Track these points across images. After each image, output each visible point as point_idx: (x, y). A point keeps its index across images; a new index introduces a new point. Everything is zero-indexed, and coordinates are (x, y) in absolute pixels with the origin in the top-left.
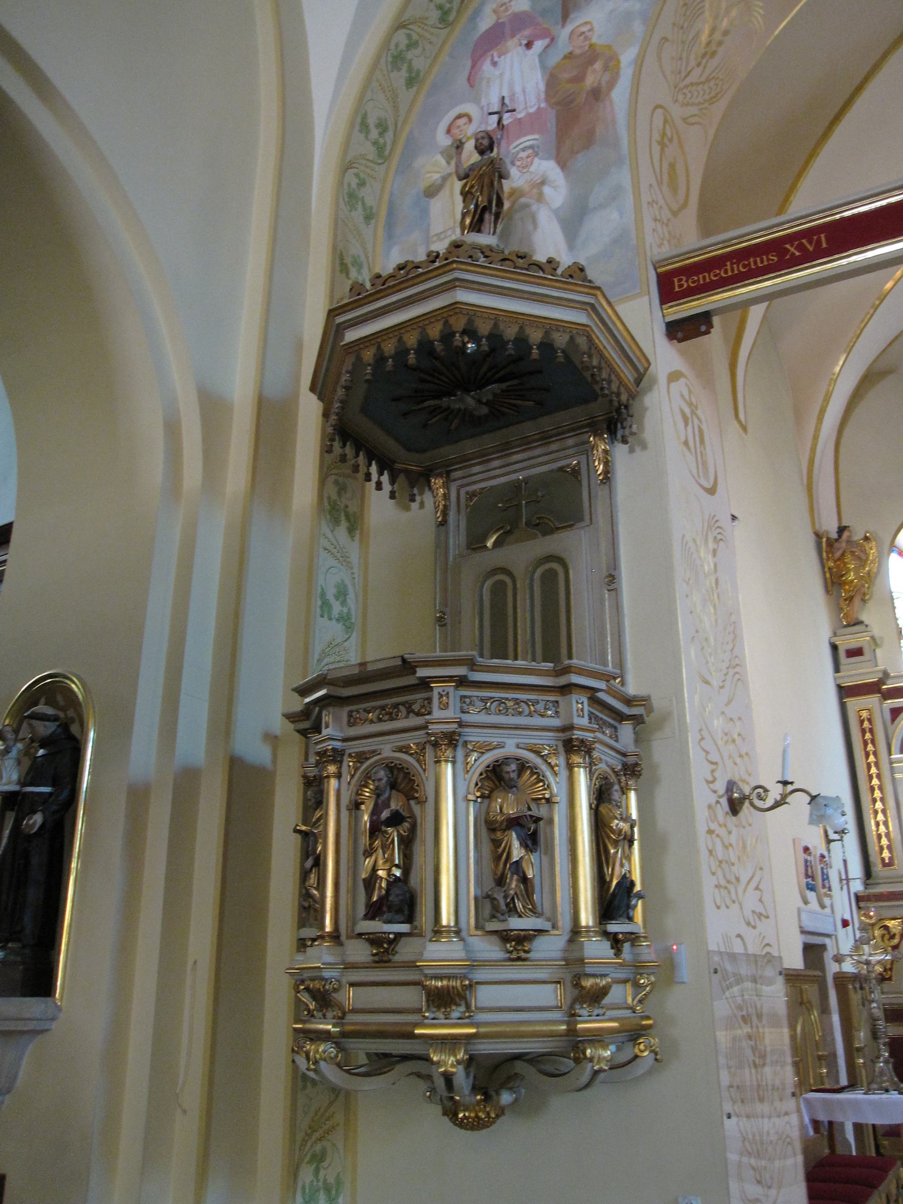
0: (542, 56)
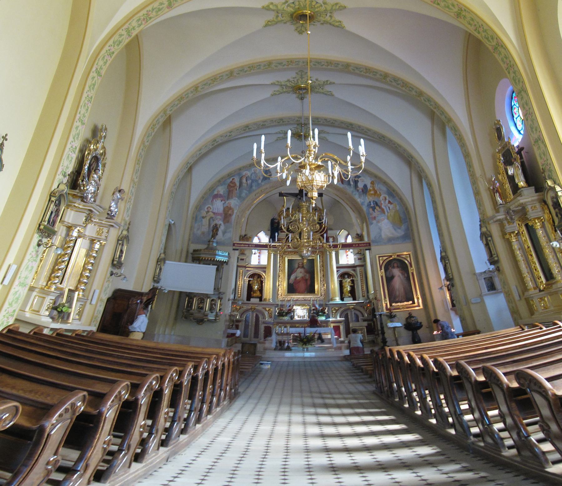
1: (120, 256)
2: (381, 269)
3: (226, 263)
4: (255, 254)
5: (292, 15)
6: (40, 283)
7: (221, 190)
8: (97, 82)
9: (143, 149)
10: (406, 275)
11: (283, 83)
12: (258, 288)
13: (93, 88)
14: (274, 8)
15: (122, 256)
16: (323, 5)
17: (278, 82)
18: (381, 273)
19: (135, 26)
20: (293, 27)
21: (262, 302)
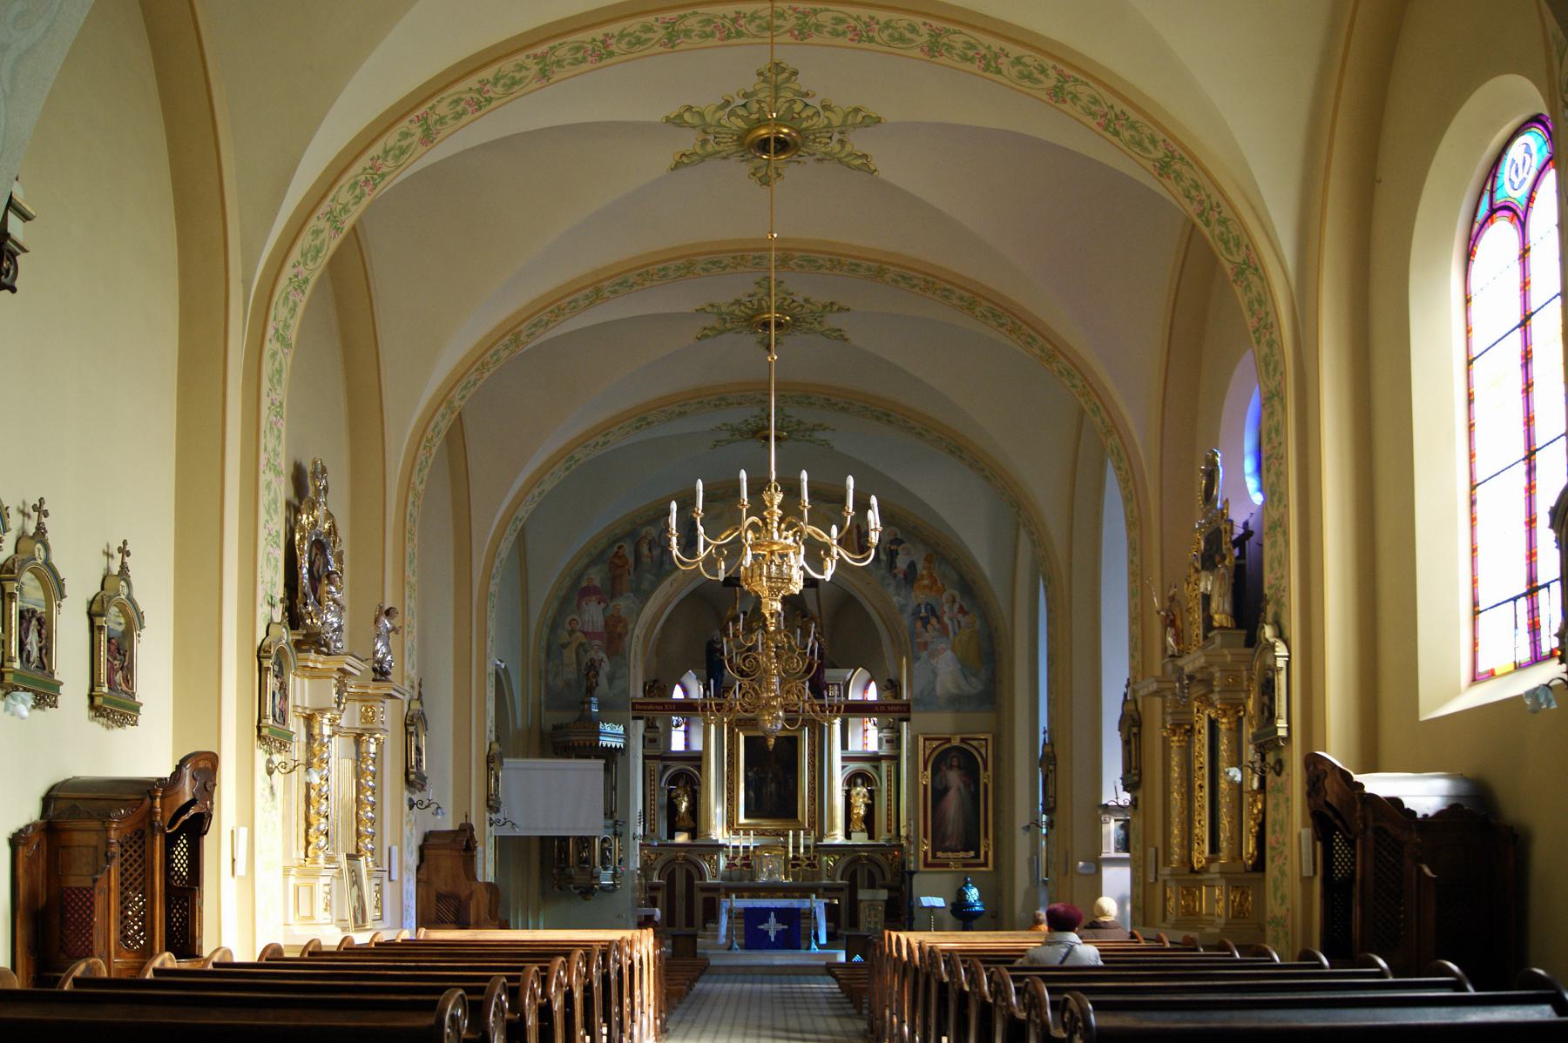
0: (604, 609)
1: (419, 761)
2: (925, 769)
3: (623, 751)
4: (678, 726)
5: (741, 138)
6: (294, 855)
7: (596, 576)
8: (284, 362)
9: (414, 502)
10: (972, 789)
11: (724, 309)
12: (687, 808)
13: (279, 381)
14: (696, 121)
15: (421, 761)
16: (822, 112)
17: (712, 306)
18: (926, 779)
19: (347, 204)
20: (746, 168)
21: (698, 842)
